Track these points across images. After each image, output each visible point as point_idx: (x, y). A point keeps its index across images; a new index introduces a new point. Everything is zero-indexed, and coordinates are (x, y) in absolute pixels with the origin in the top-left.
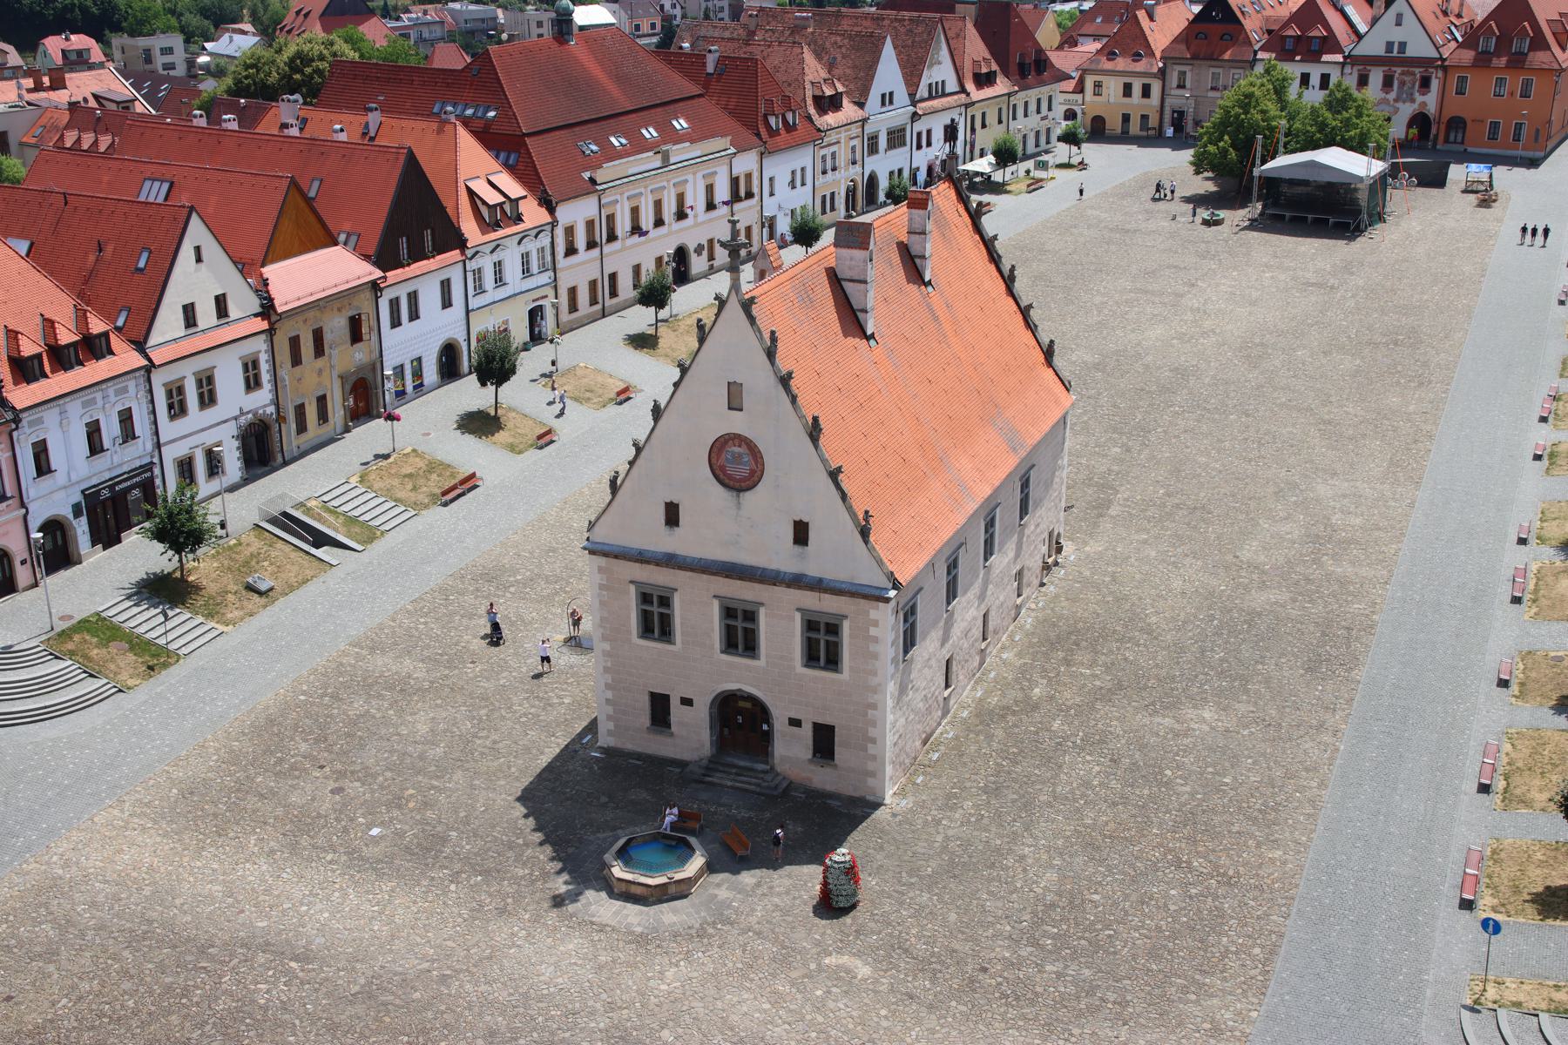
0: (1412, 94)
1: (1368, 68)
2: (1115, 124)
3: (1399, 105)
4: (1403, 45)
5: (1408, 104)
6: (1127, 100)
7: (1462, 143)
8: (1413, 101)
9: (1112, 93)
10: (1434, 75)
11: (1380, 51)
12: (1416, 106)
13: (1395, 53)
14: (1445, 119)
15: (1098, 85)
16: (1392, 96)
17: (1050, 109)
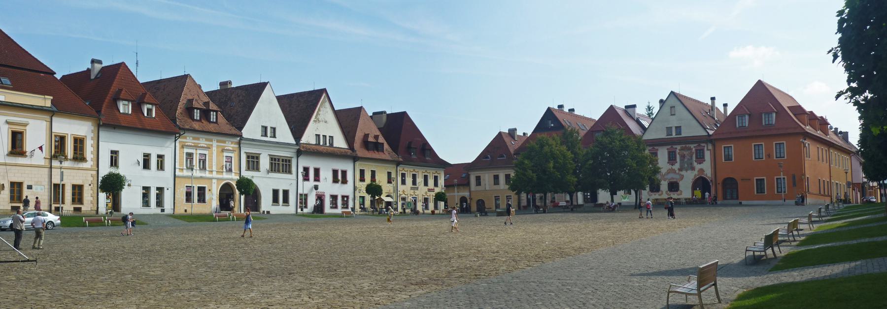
0: (691, 164)
1: (656, 148)
2: (490, 204)
3: (683, 173)
4: (678, 129)
5: (689, 172)
6: (496, 187)
7: (737, 198)
8: (693, 169)
9: (487, 183)
10: (706, 148)
11: (663, 135)
12: (696, 172)
13: (674, 135)
14: (720, 180)
15: (478, 179)
16: (677, 166)
17: (436, 185)
